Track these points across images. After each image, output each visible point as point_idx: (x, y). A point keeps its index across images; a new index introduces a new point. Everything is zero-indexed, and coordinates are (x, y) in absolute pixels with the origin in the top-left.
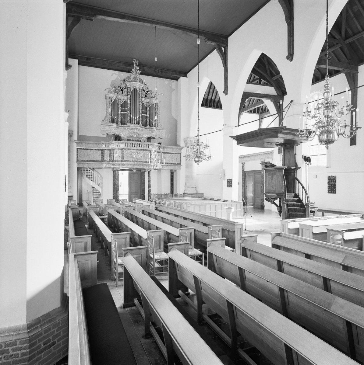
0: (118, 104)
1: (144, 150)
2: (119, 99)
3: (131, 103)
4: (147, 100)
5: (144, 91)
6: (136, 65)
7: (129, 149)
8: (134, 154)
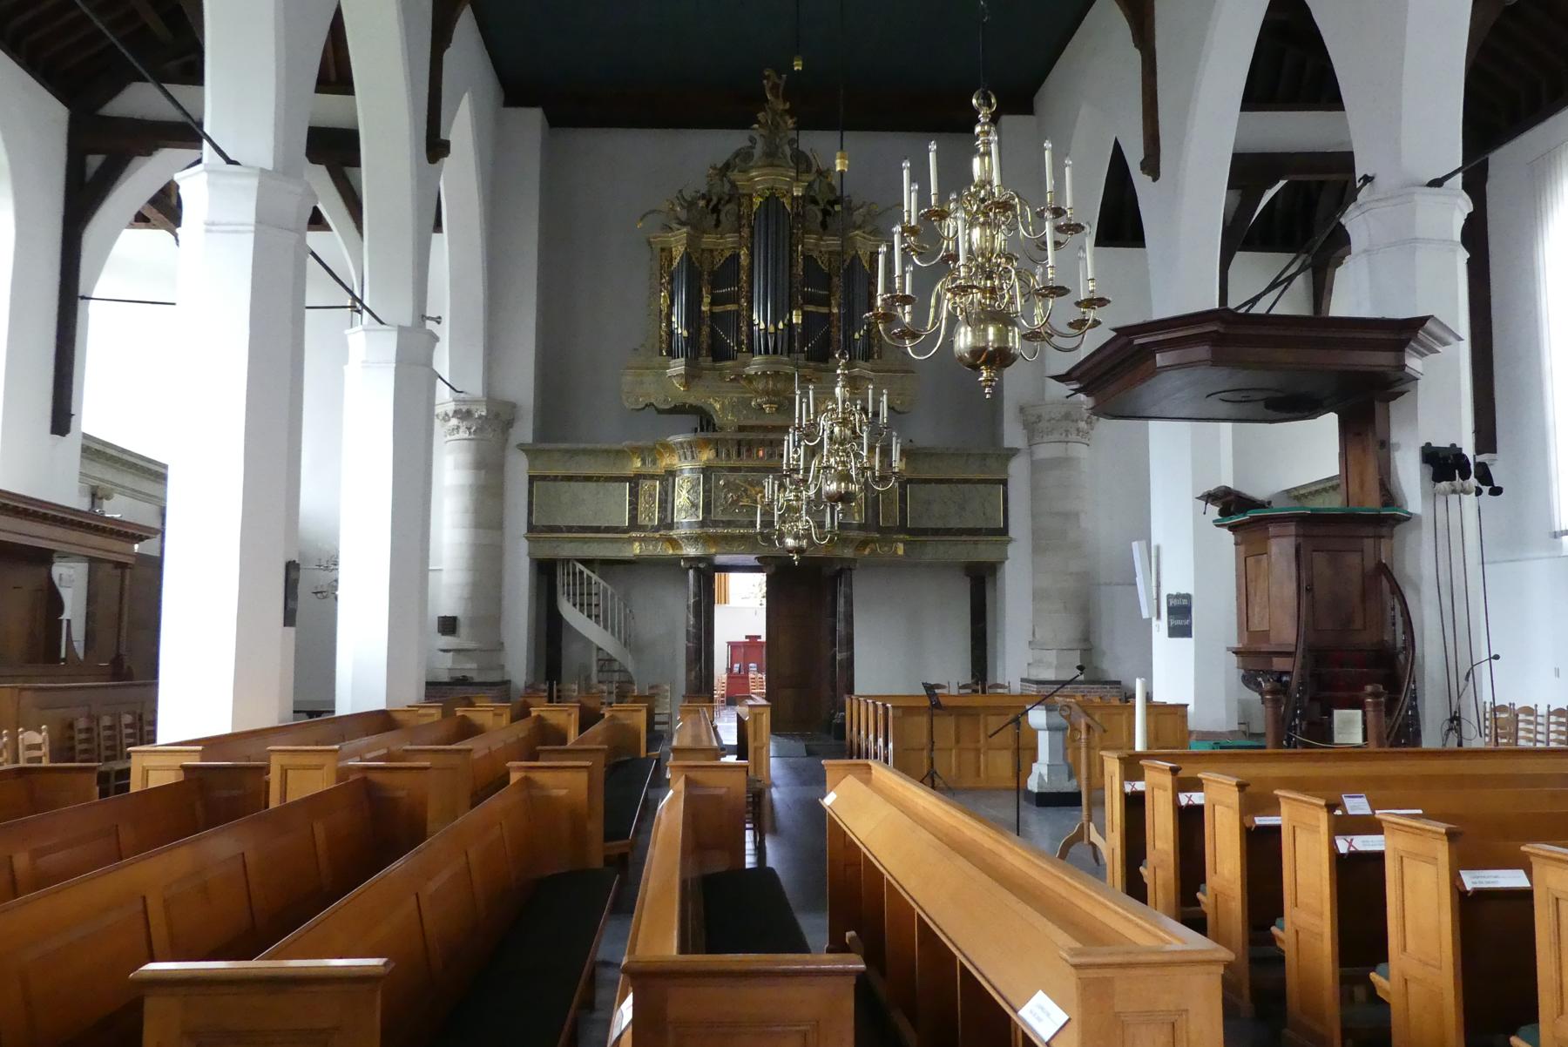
0: (701, 274)
3: (752, 263)
4: (832, 242)
5: (814, 201)
6: (777, 97)
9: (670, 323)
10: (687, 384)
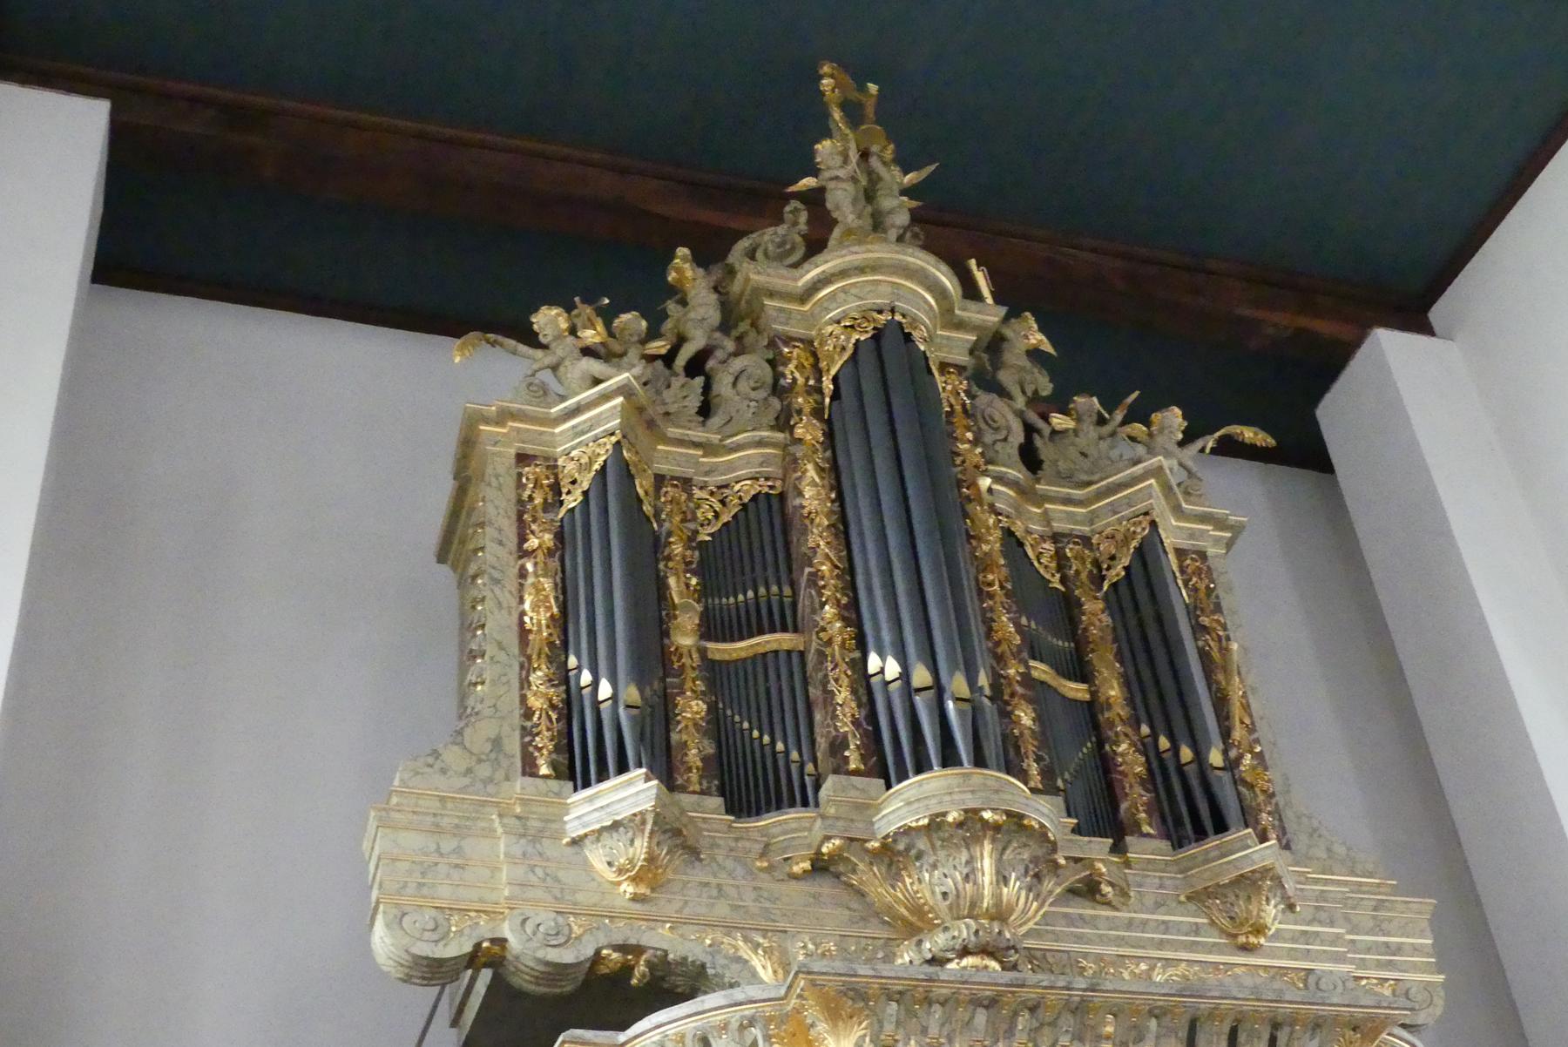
2: (660, 480)
9: (563, 678)
10: (649, 874)
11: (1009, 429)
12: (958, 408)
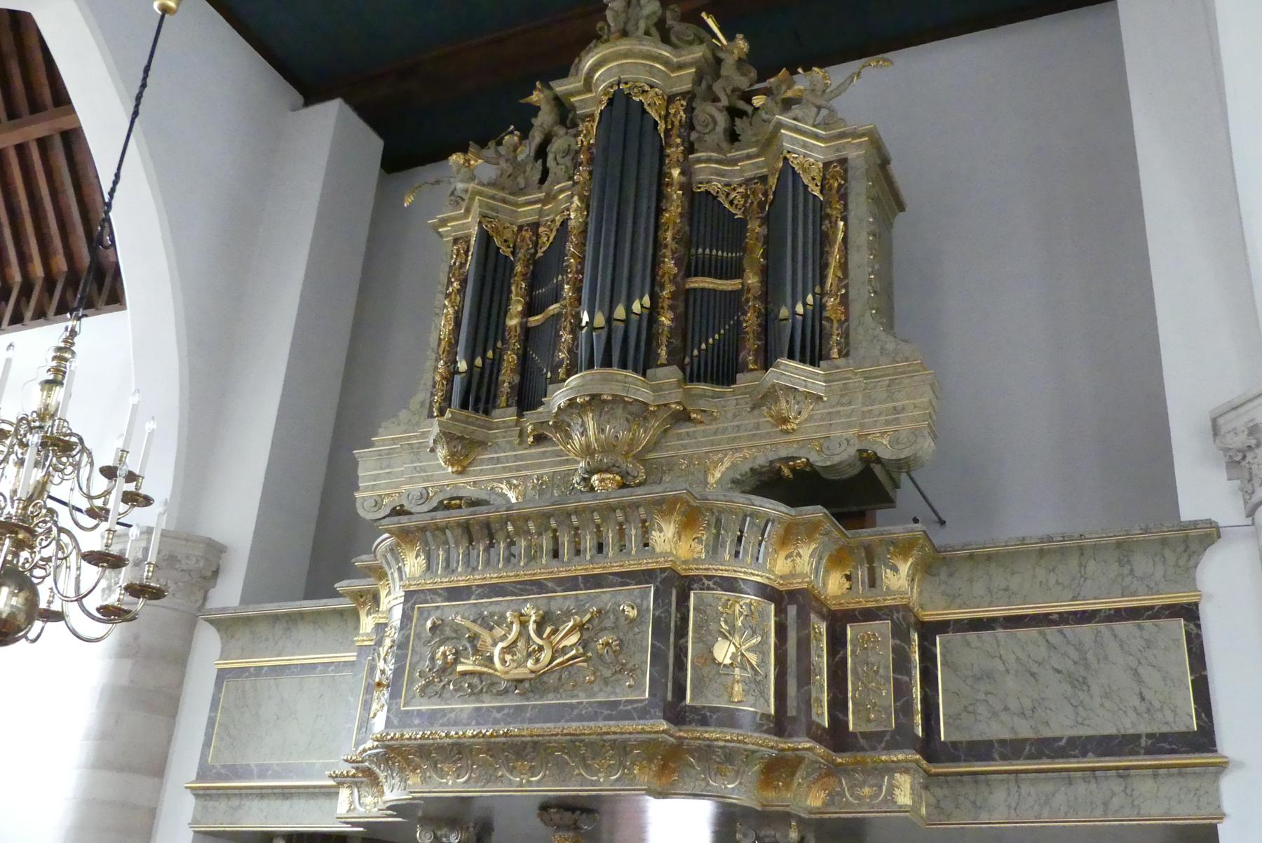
1: (595, 581)
2: (520, 228)
7: (455, 594)
8: (499, 632)
11: (715, 123)
12: (677, 123)
